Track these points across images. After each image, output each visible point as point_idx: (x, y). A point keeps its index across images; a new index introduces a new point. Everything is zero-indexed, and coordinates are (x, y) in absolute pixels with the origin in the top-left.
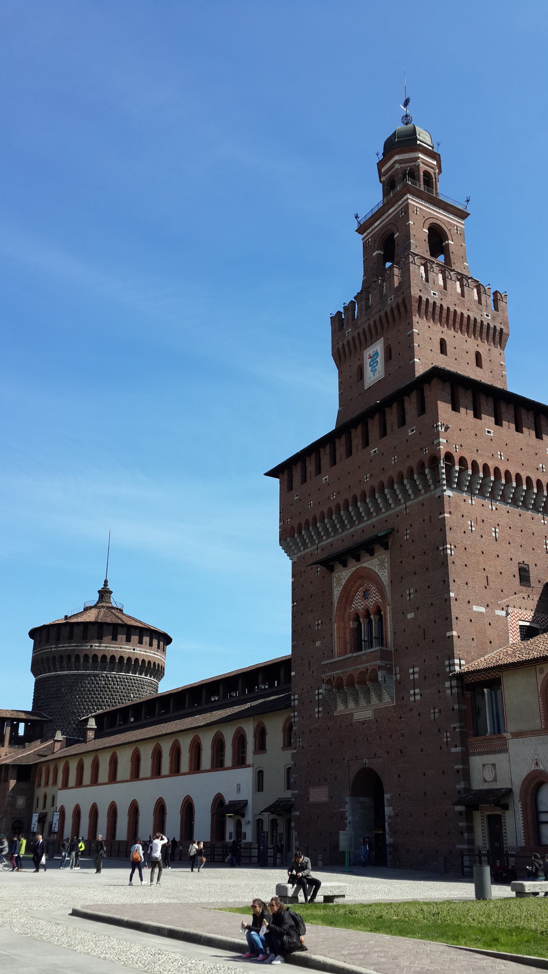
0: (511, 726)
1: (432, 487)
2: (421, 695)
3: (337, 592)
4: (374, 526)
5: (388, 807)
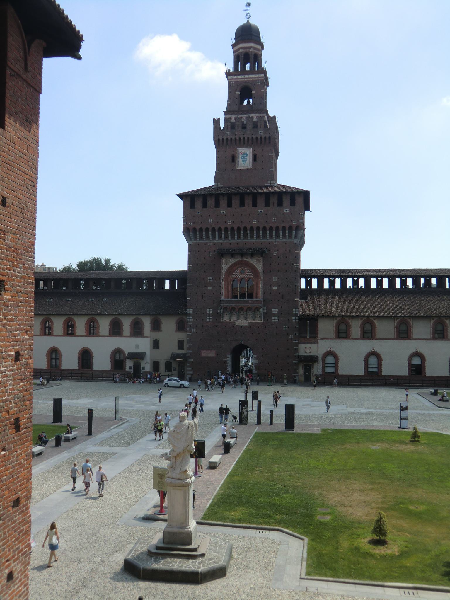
0: (320, 335)
1: (293, 238)
2: (278, 320)
3: (225, 267)
4: (253, 244)
5: (255, 360)
